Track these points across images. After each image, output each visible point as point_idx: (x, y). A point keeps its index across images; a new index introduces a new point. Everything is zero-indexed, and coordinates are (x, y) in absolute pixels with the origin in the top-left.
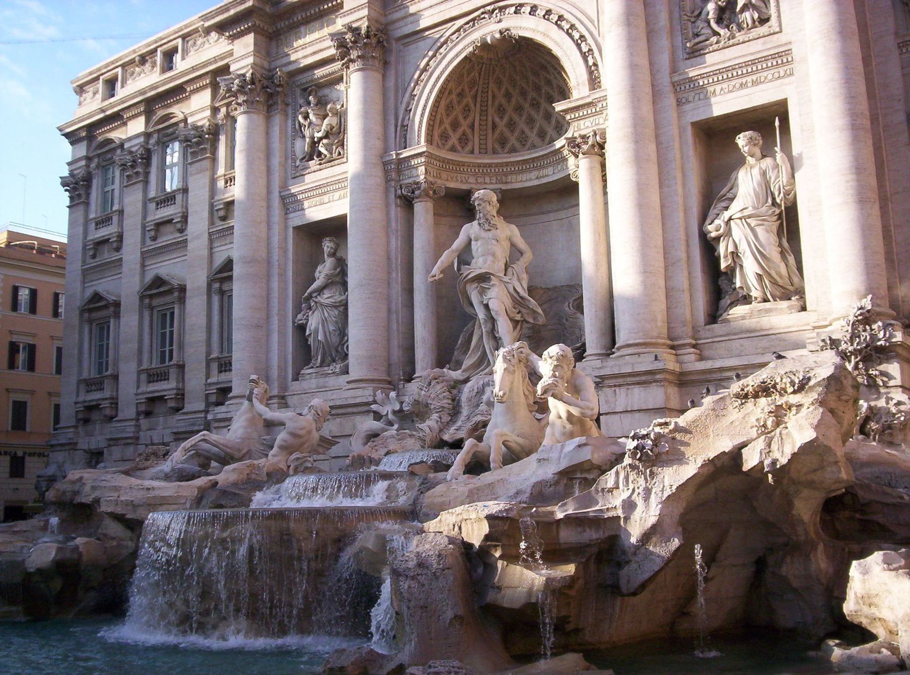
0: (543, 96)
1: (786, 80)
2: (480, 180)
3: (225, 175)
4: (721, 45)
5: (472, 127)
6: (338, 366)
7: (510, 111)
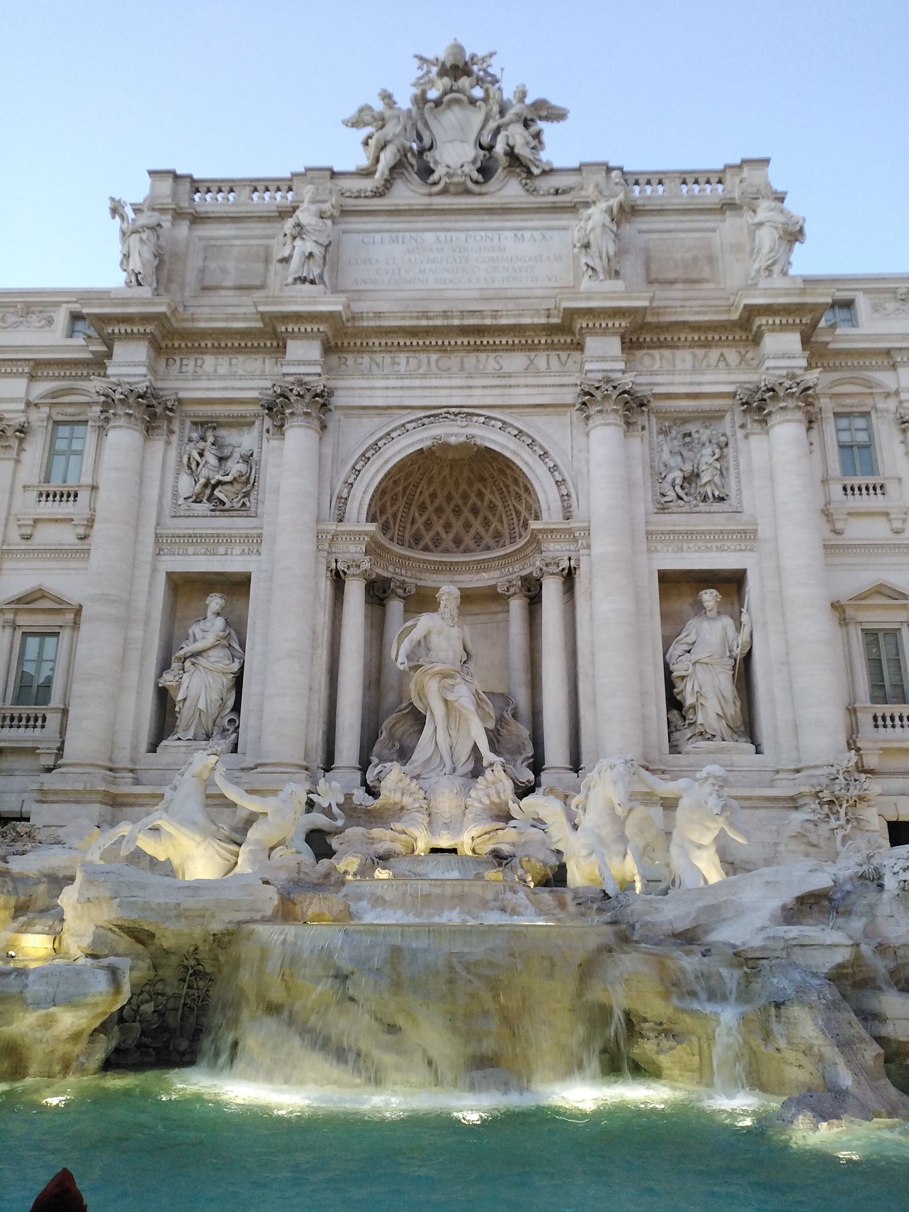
0: (469, 506)
1: (747, 554)
2: (398, 570)
3: (38, 487)
5: (395, 516)
6: (223, 741)
7: (431, 509)
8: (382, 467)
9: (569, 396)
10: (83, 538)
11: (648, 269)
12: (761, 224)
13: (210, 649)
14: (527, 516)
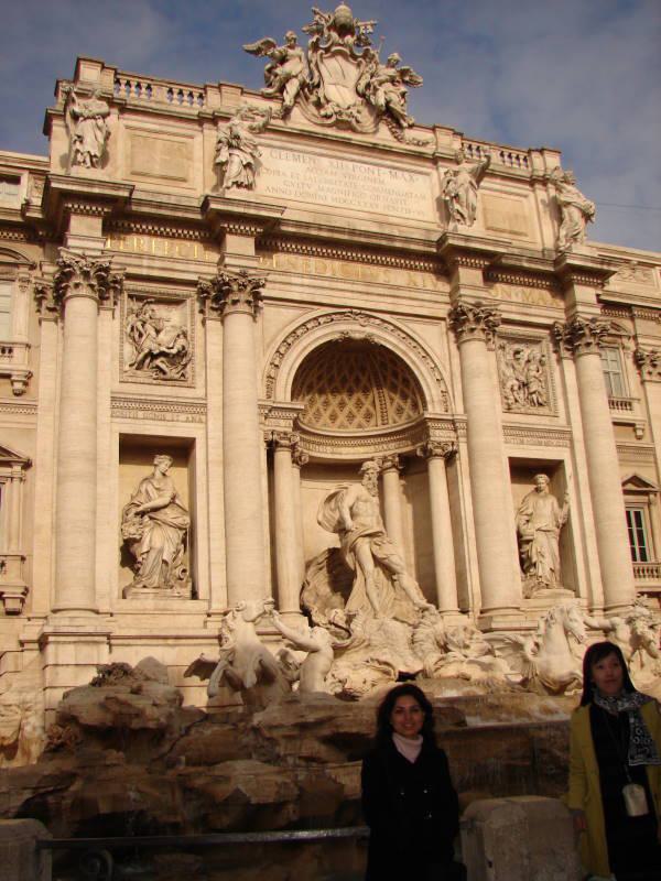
4: (523, 410)
8: (301, 353)
9: (443, 311)
10: (18, 394)
11: (486, 220)
12: (568, 204)
13: (165, 507)
14: (402, 404)
